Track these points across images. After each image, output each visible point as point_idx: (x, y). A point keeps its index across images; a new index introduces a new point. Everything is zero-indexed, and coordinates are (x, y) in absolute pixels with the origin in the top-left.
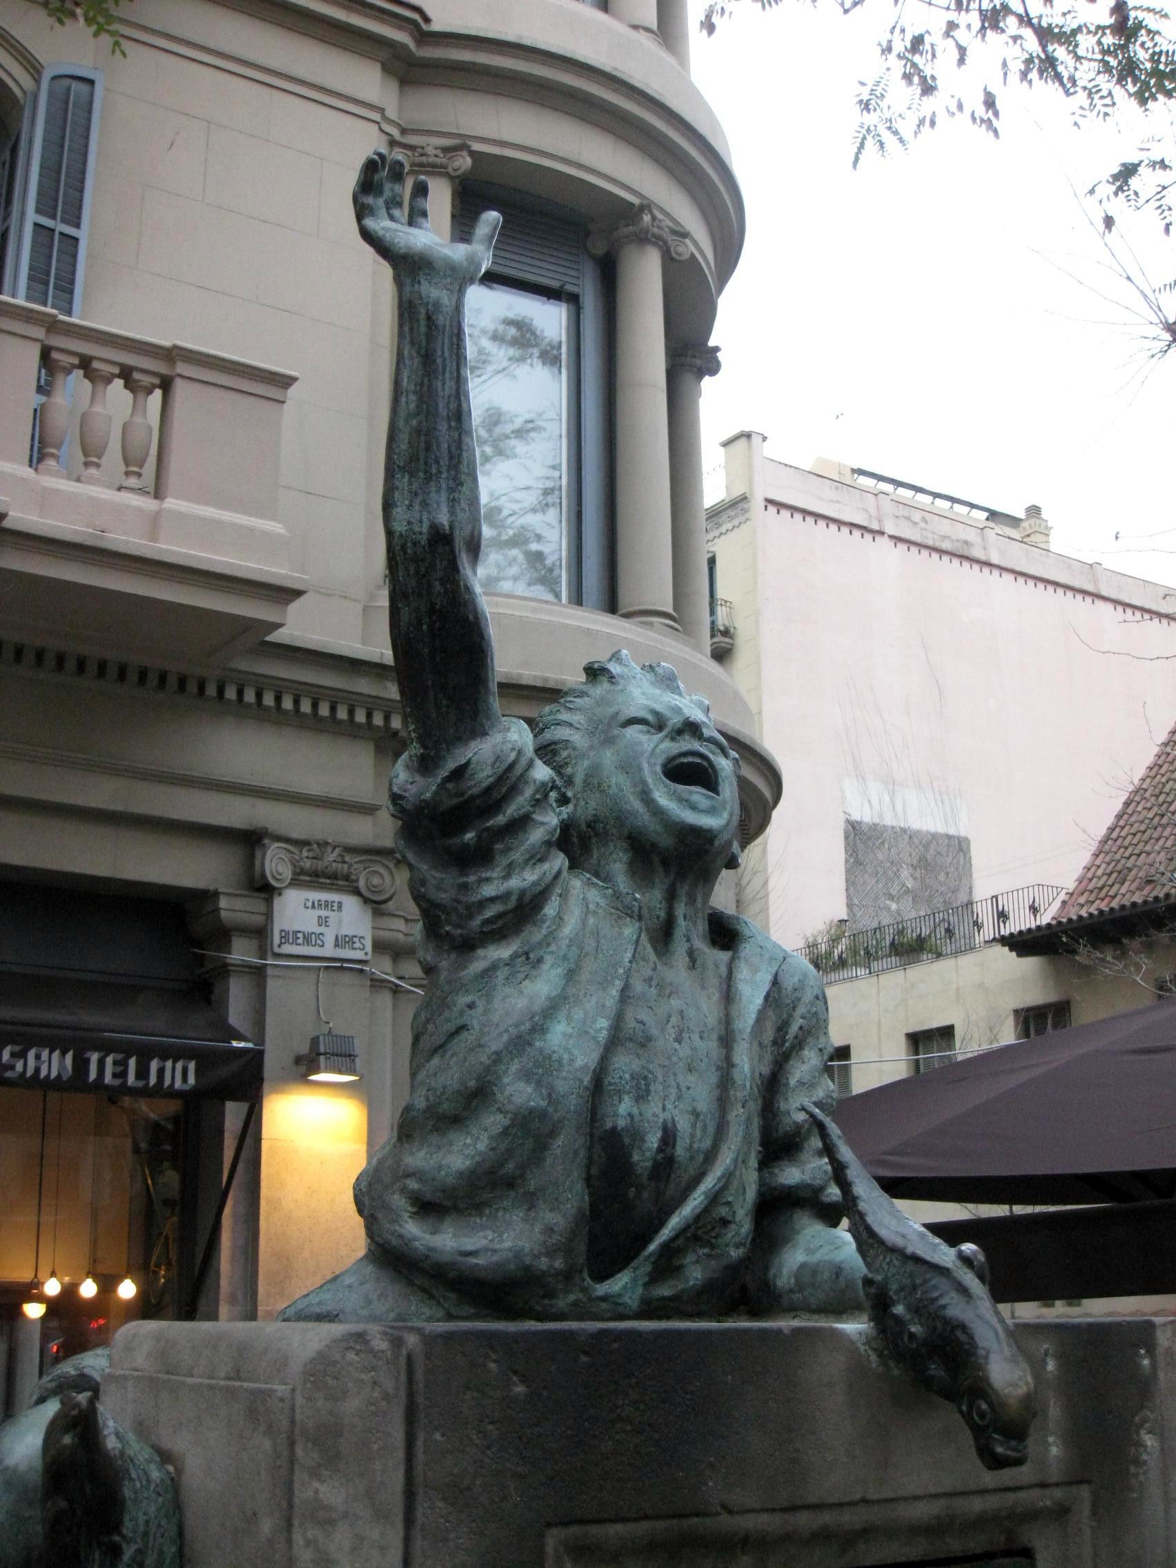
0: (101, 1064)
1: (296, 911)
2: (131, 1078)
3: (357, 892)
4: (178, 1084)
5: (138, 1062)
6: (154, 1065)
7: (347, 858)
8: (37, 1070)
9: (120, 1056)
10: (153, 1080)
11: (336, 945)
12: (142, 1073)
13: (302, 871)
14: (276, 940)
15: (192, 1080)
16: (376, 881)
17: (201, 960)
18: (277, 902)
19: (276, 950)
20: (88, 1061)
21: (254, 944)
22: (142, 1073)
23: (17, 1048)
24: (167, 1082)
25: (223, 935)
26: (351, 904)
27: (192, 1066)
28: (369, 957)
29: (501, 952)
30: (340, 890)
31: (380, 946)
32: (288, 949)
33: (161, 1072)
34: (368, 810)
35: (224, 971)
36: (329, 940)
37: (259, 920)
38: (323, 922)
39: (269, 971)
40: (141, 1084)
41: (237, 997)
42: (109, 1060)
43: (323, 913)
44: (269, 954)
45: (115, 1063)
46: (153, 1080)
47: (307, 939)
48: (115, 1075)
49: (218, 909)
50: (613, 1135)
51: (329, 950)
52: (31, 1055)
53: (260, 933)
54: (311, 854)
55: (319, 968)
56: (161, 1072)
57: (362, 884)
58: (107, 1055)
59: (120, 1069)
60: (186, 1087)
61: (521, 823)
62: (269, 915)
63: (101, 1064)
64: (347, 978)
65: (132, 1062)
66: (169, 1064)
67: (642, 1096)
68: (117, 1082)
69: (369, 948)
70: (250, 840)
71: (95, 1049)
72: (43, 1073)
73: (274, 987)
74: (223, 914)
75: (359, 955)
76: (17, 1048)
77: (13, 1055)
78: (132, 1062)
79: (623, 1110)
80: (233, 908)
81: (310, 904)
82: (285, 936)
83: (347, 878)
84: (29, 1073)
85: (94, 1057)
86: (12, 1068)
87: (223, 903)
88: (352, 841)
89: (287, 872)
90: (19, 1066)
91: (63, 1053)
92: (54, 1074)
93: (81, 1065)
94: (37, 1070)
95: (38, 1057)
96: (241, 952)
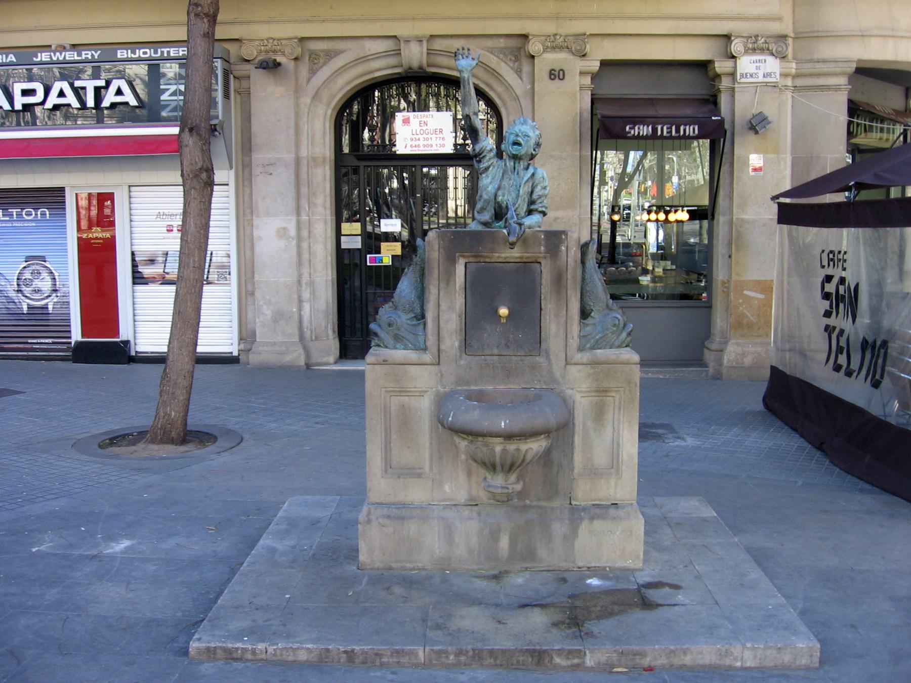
1: (747, 65)
14: (738, 77)
16: (780, 49)
17: (714, 86)
18: (738, 61)
21: (730, 78)
25: (718, 76)
26: (770, 59)
29: (484, 175)
31: (784, 75)
32: (743, 80)
34: (779, 19)
35: (719, 91)
36: (761, 75)
37: (730, 70)
38: (758, 68)
41: (724, 100)
43: (758, 65)
47: (751, 76)
50: (498, 203)
51: (761, 79)
53: (733, 75)
61: (484, 157)
62: (735, 67)
67: (503, 196)
69: (778, 76)
70: (727, 37)
74: (717, 69)
75: (774, 80)
79: (500, 199)
80: (722, 66)
82: (742, 76)
83: (768, 49)
87: (717, 65)
88: (769, 33)
96: (725, 83)
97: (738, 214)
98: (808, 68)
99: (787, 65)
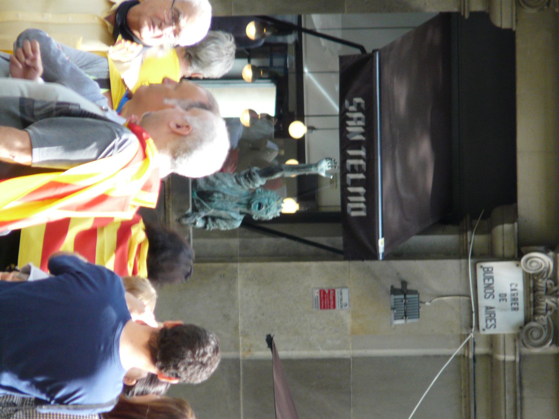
0: (359, 157)
2: (351, 176)
3: (527, 320)
4: (350, 206)
5: (361, 180)
6: (361, 190)
7: (549, 313)
8: (351, 119)
9: (364, 168)
10: (351, 189)
11: (487, 308)
12: (355, 183)
13: (535, 281)
15: (354, 214)
16: (536, 334)
19: (478, 265)
20: (359, 148)
22: (355, 183)
23: (363, 106)
24: (351, 199)
26: (519, 316)
27: (363, 214)
28: (482, 332)
30: (526, 308)
31: (492, 340)
32: (480, 273)
33: (357, 194)
36: (490, 302)
37: (499, 251)
38: (503, 297)
39: (463, 261)
40: (349, 182)
41: (444, 239)
42: (362, 162)
44: (476, 260)
45: (360, 166)
46: (351, 189)
47: (489, 286)
48: (352, 166)
49: (503, 223)
51: (483, 302)
52: (360, 115)
54: (549, 287)
55: (470, 297)
56: (357, 194)
57: (533, 324)
58: (364, 160)
59: (357, 169)
60: (349, 211)
62: (503, 258)
63: (359, 157)
64: (465, 317)
65: (361, 176)
66: (363, 199)
68: (348, 167)
71: (368, 153)
72: (349, 123)
73: (452, 265)
74: (500, 228)
75: (482, 324)
76: (363, 106)
77: (359, 105)
78: (361, 176)
80: (504, 232)
81: (513, 287)
82: (488, 271)
83: (535, 313)
84: (348, 114)
85: (362, 153)
86: (351, 104)
89: (533, 269)
90: (352, 108)
91: (363, 134)
92: (349, 129)
93: (357, 145)
94: (351, 119)
95: (359, 119)
97: (244, 269)
98: (507, 382)
99: (510, 344)
